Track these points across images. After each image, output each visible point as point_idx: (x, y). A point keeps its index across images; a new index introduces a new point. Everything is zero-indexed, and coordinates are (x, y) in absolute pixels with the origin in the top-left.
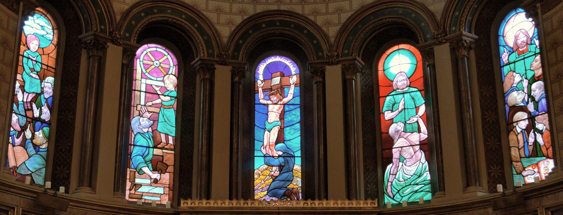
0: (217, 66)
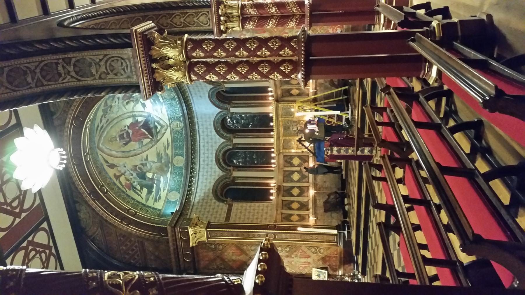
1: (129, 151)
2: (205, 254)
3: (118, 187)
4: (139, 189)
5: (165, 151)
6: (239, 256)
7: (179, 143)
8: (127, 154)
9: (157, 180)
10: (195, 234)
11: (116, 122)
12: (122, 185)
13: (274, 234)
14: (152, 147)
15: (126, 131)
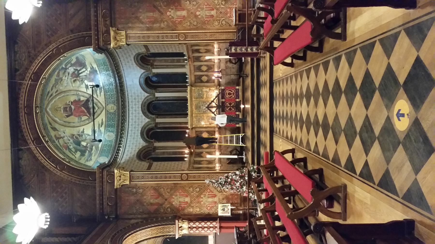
0: (156, 122)
1: (70, 123)
2: (127, 198)
3: (57, 144)
4: (74, 151)
5: (99, 128)
6: (157, 198)
7: (111, 122)
8: (67, 124)
9: (90, 148)
10: (120, 177)
11: (63, 95)
12: (60, 145)
13: (187, 174)
14: (88, 123)
15: (69, 106)
